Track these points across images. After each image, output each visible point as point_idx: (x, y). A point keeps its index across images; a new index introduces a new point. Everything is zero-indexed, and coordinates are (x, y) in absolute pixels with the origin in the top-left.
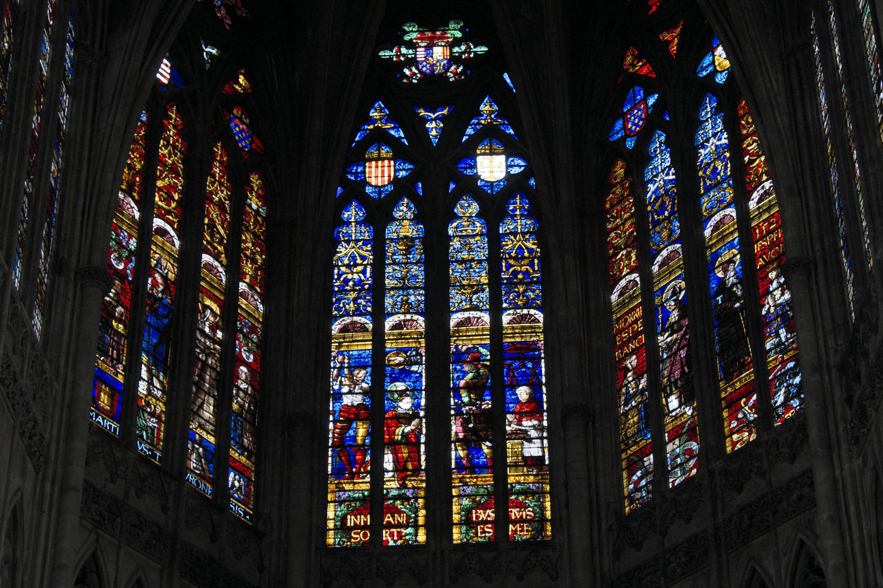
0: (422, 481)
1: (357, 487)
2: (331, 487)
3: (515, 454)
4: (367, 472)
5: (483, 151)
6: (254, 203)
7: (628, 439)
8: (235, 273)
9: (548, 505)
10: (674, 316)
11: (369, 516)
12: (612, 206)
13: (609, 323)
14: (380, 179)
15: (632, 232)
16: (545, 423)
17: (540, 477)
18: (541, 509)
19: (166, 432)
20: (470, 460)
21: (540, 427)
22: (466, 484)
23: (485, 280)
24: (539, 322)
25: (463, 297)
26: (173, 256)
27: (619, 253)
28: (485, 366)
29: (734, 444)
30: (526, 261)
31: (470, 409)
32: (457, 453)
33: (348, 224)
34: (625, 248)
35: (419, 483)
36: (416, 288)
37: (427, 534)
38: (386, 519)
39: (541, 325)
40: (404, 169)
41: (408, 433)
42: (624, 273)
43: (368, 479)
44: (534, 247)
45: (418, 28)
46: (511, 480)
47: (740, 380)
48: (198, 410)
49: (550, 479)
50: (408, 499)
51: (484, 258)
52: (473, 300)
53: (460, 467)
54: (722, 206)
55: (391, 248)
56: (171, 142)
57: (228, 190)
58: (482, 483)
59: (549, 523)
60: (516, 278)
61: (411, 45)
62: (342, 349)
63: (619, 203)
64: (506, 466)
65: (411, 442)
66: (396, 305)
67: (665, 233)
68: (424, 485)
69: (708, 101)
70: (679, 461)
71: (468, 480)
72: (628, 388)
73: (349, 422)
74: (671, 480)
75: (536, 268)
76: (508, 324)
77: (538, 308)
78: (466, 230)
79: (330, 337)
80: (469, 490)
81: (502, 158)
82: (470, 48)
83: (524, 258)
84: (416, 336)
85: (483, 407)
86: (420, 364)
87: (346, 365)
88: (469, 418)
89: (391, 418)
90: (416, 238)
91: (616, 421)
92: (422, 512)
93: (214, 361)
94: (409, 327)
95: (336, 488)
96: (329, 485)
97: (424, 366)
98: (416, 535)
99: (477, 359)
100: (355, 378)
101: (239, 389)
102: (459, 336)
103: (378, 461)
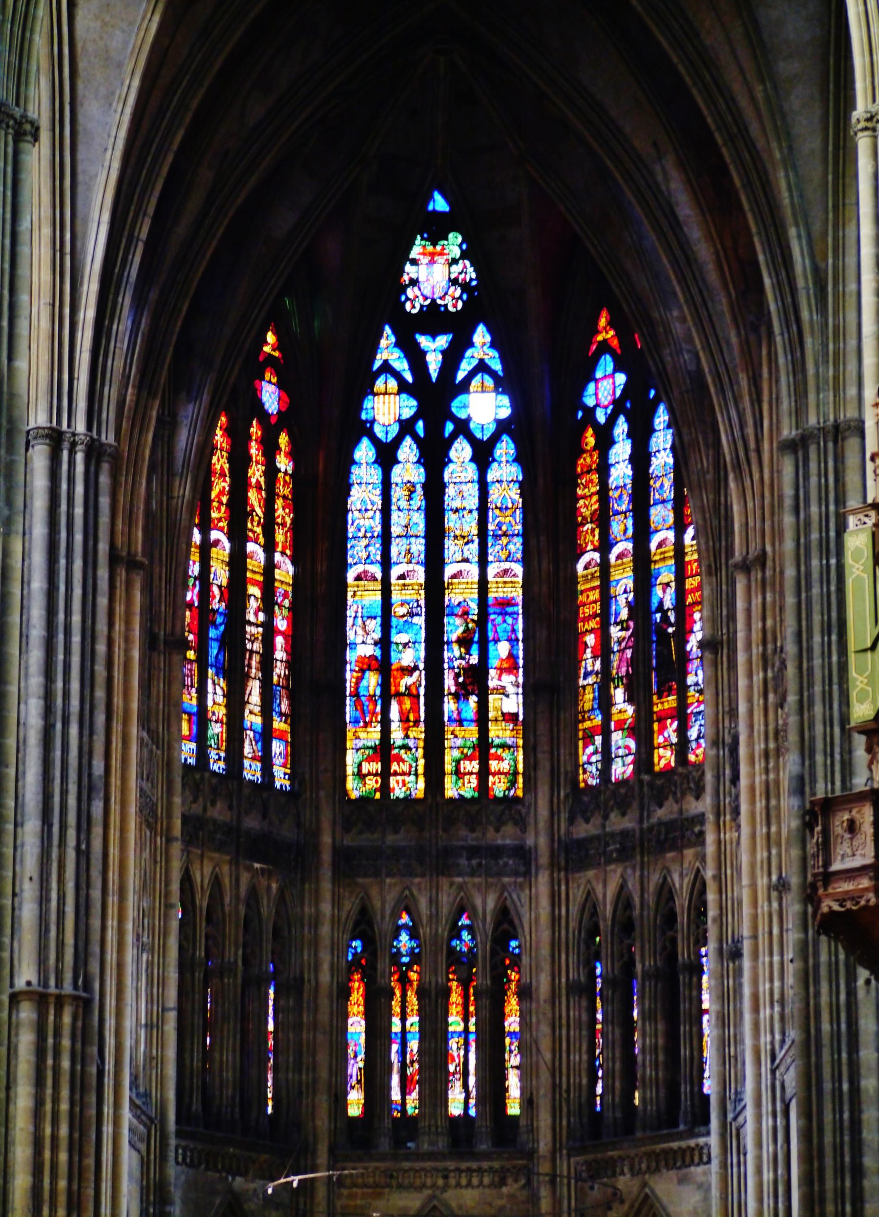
2: (349, 735)
3: (496, 709)
4: (376, 721)
6: (283, 463)
7: (584, 712)
8: (270, 547)
9: (520, 758)
10: (624, 614)
11: (379, 764)
12: (582, 473)
13: (574, 593)
15: (595, 510)
16: (521, 680)
20: (459, 713)
22: (456, 737)
23: (475, 531)
25: (457, 548)
28: (472, 620)
29: (660, 758)
30: (509, 512)
32: (449, 706)
33: (359, 464)
34: (591, 522)
35: (418, 733)
36: (417, 537)
37: (426, 782)
39: (520, 579)
43: (379, 728)
44: (517, 497)
46: (492, 734)
50: (410, 749)
54: (665, 527)
55: (398, 494)
60: (500, 529)
61: (414, 262)
62: (356, 598)
63: (588, 472)
64: (487, 720)
67: (622, 527)
68: (423, 736)
70: (621, 752)
73: (362, 671)
75: (518, 521)
77: (517, 561)
79: (345, 585)
80: (459, 742)
81: (494, 394)
83: (507, 508)
86: (421, 615)
87: (359, 614)
88: (460, 672)
89: (397, 670)
91: (576, 692)
92: (422, 762)
98: (417, 783)
99: (466, 613)
101: (277, 660)
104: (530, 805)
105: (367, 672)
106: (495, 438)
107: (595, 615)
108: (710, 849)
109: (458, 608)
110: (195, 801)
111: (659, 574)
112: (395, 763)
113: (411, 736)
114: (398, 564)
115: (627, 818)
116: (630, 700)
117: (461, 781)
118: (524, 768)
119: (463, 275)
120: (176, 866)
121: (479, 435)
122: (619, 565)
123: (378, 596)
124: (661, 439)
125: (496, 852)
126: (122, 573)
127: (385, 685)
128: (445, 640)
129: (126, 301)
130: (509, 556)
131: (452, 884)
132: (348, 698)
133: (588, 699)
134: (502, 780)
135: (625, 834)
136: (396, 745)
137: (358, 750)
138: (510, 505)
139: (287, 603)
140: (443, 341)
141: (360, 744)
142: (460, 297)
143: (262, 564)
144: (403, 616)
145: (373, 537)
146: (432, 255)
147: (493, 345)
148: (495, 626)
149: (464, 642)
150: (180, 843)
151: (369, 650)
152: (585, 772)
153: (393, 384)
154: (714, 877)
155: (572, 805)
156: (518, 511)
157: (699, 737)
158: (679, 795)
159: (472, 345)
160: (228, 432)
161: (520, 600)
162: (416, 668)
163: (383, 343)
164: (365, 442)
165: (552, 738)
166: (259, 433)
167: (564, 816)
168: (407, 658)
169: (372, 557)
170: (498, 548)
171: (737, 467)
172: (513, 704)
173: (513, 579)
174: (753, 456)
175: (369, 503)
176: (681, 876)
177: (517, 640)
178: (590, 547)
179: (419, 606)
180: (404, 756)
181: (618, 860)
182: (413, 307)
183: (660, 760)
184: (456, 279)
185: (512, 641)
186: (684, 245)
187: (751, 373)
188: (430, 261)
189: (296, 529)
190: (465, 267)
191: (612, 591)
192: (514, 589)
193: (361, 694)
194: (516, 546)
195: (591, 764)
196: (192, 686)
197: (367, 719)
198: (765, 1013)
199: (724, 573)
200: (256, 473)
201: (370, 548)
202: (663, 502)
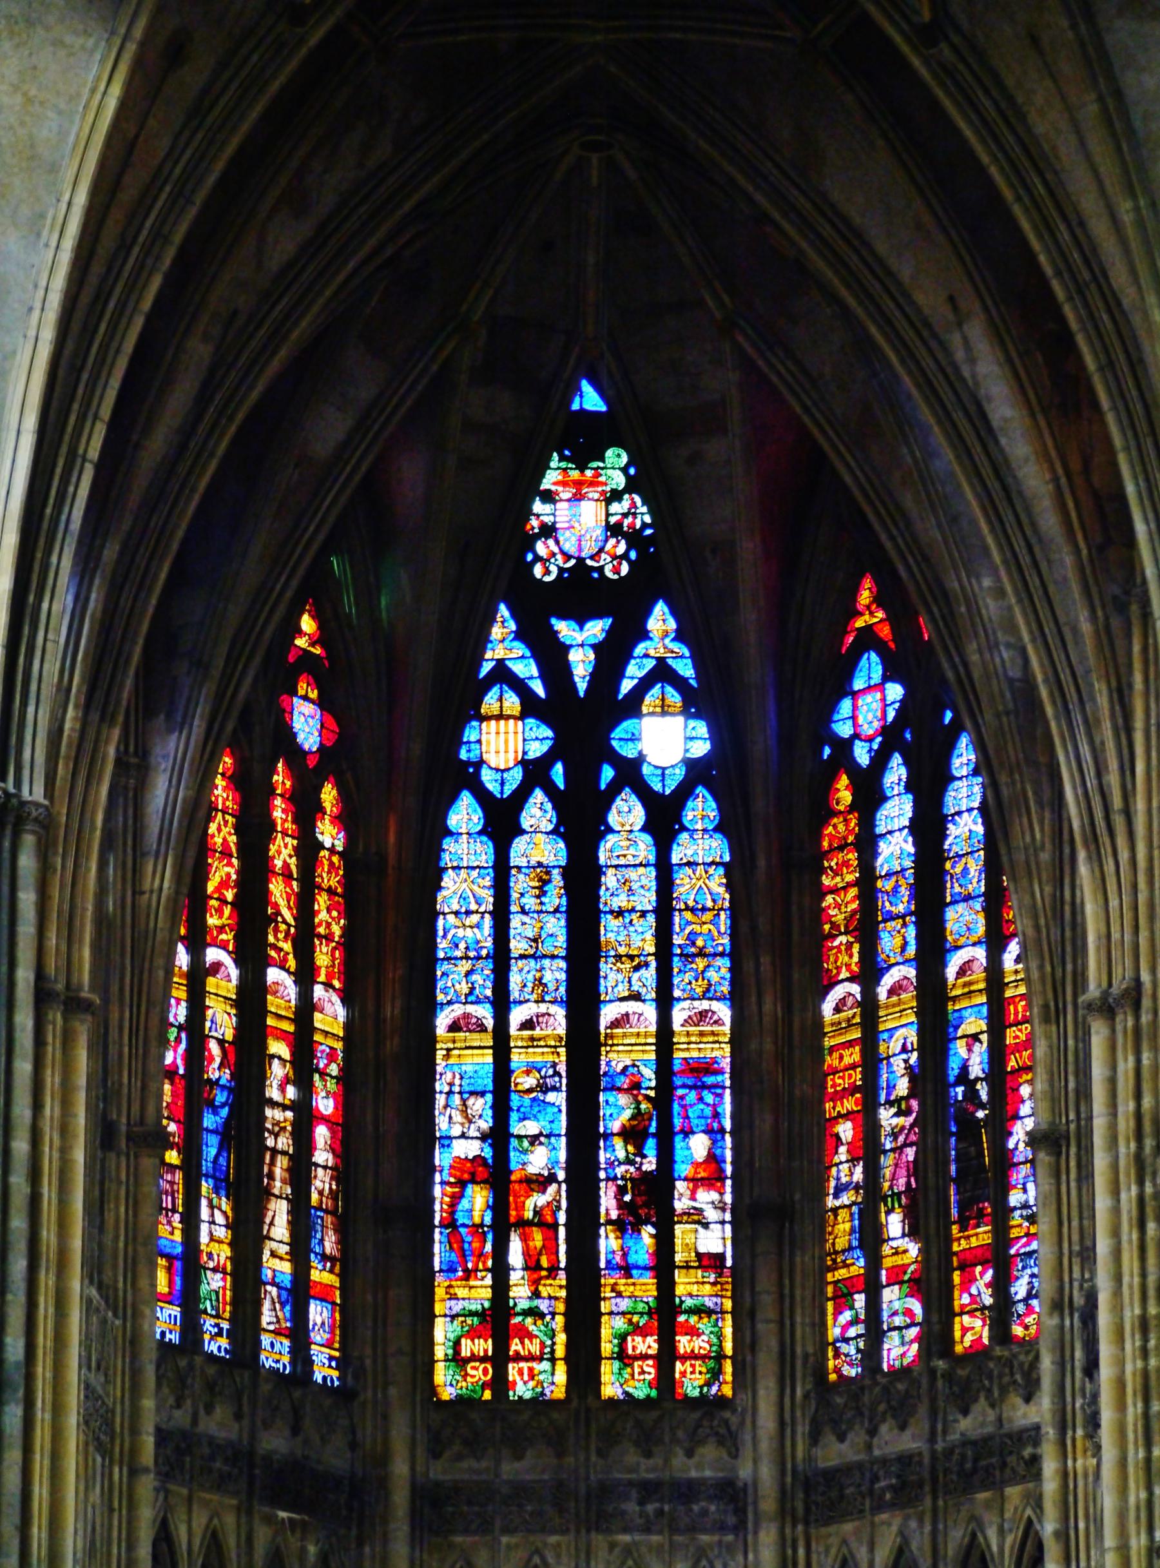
0: (561, 1287)
1: (474, 1293)
2: (440, 1292)
4: (486, 1270)
5: (651, 709)
6: (328, 834)
7: (836, 1253)
8: (305, 976)
9: (728, 1331)
10: (902, 1087)
11: (490, 1341)
13: (818, 1053)
14: (502, 754)
15: (854, 912)
16: (728, 1198)
17: (719, 1287)
18: (719, 1338)
19: (234, 1289)
20: (625, 1255)
21: (721, 1205)
22: (619, 1295)
24: (723, 1024)
25: (620, 977)
26: (230, 999)
27: (836, 936)
28: (647, 1097)
29: (965, 1330)
30: (708, 916)
31: (626, 1172)
32: (608, 1243)
34: (846, 933)
35: (556, 1288)
36: (553, 957)
37: (569, 1373)
38: (513, 1348)
39: (727, 1029)
40: (537, 739)
41: (542, 1208)
42: (842, 976)
43: (488, 1281)
44: (722, 890)
45: (560, 461)
46: (680, 1290)
47: (977, 1235)
48: (269, 1231)
49: (733, 1291)
50: (542, 1316)
51: (651, 908)
52: (633, 982)
55: (520, 884)
56: (220, 807)
57: (293, 838)
58: (641, 1294)
59: (729, 1362)
60: (693, 944)
61: (549, 497)
62: (451, 1061)
63: (841, 848)
64: (673, 1266)
66: (525, 986)
67: (898, 941)
69: (964, 745)
70: (898, 1321)
71: (622, 1288)
72: (839, 1171)
73: (462, 1184)
74: (886, 1346)
76: (682, 1025)
78: (625, 856)
79: (432, 1039)
80: (624, 1304)
81: (680, 719)
82: (636, 508)
83: (704, 909)
84: (553, 1043)
85: (644, 1168)
87: (456, 1089)
88: (625, 1186)
89: (520, 1181)
90: (554, 867)
91: (821, 1220)
92: (561, 1338)
93: (285, 1141)
94: (544, 1026)
95: (447, 1293)
96: (437, 1289)
97: (564, 1094)
98: (553, 1374)
99: (636, 1086)
100: (469, 1111)
101: (317, 1165)
102: (612, 1046)
104: (744, 1410)
105: (470, 1186)
106: (684, 792)
107: (852, 1090)
108: (1050, 1486)
109: (622, 1078)
110: (178, 1406)
111: (961, 1020)
112: (517, 1340)
113: (544, 1294)
114: (521, 1003)
115: (908, 1433)
116: (912, 1232)
117: (629, 1370)
118: (734, 1348)
119: (630, 519)
120: (146, 1515)
121: (657, 787)
122: (894, 1006)
123: (489, 1058)
124: (964, 792)
125: (687, 1491)
126: (56, 1017)
127: (499, 1207)
128: (602, 1130)
129: (64, 561)
130: (708, 990)
131: (612, 1546)
132: (437, 1230)
133: (842, 1231)
134: (698, 1369)
135: (906, 1460)
136: (518, 1309)
137: (453, 1317)
138: (710, 904)
139: (334, 1069)
140: (596, 629)
141: (457, 1307)
142: (625, 556)
143: (293, 1002)
144: (529, 1091)
145: (478, 958)
146: (578, 484)
147: (679, 637)
148: (685, 1107)
149: (634, 1134)
150: (152, 1476)
151: (470, 1149)
152: (837, 1354)
153: (512, 702)
154: (1057, 1534)
155: (817, 1411)
156: (723, 915)
157: (1030, 1296)
158: (996, 1394)
159: (645, 635)
160: (236, 781)
161: (726, 1064)
162: (552, 1178)
163: (496, 632)
164: (466, 799)
165: (781, 1296)
166: (288, 784)
167: (802, 1429)
168: (537, 1161)
169: (477, 992)
170: (689, 976)
171: (1092, 840)
173: (715, 1028)
174: (1119, 821)
175: (472, 900)
176: (1001, 1532)
177: (722, 1131)
178: (844, 974)
179: (557, 1074)
180: (531, 1328)
181: (893, 1506)
182: (547, 572)
183: (963, 1336)
184: (619, 524)
185: (714, 1133)
186: (1001, 468)
187: (1114, 684)
188: (574, 495)
189: (349, 944)
190: (633, 505)
191: (882, 1048)
192: (717, 1046)
193: (460, 1222)
194: (720, 973)
195: (847, 1341)
196: (174, 1210)
197: (470, 1265)
199: (1070, 1017)
200: (283, 851)
201: (474, 977)
202: (968, 898)
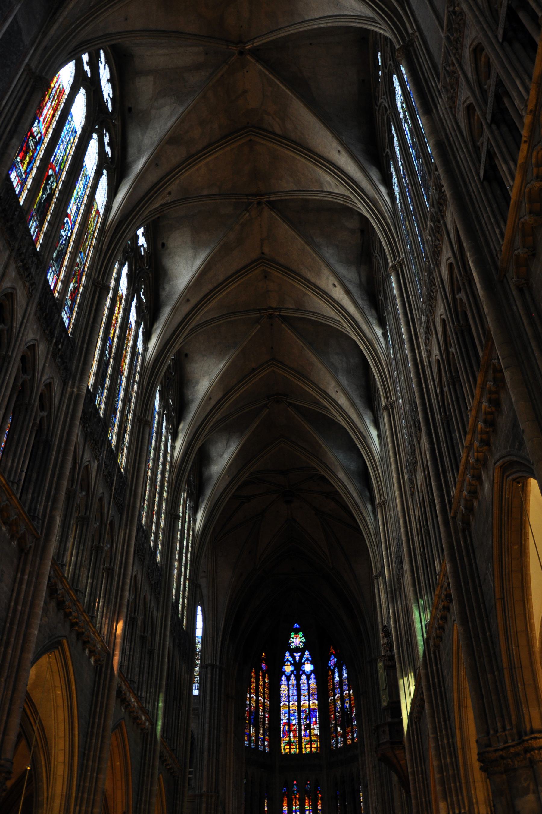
6: (267, 681)
8: (264, 699)
9: (319, 744)
10: (339, 710)
32: (303, 733)
35: (297, 739)
53: (304, 736)
55: (291, 686)
61: (293, 638)
65: (295, 730)
103: (290, 734)
106: (311, 674)
107: (332, 711)
116: (341, 729)
123: (287, 709)
127: (289, 728)
140: (299, 654)
149: (306, 718)
151: (285, 721)
153: (289, 663)
163: (287, 655)
168: (294, 722)
172: (317, 732)
185: (316, 718)
189: (270, 695)
198: (374, 798)
200: (261, 683)
